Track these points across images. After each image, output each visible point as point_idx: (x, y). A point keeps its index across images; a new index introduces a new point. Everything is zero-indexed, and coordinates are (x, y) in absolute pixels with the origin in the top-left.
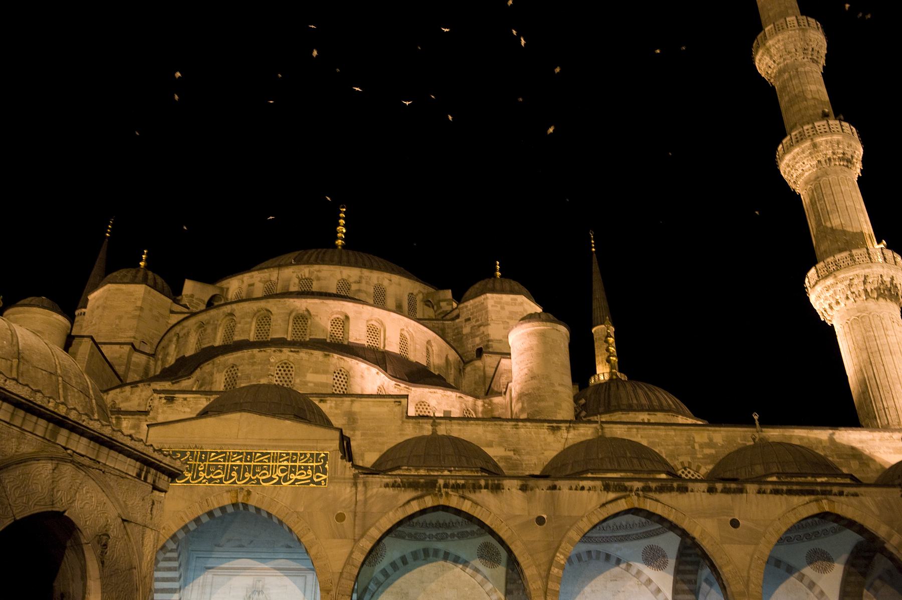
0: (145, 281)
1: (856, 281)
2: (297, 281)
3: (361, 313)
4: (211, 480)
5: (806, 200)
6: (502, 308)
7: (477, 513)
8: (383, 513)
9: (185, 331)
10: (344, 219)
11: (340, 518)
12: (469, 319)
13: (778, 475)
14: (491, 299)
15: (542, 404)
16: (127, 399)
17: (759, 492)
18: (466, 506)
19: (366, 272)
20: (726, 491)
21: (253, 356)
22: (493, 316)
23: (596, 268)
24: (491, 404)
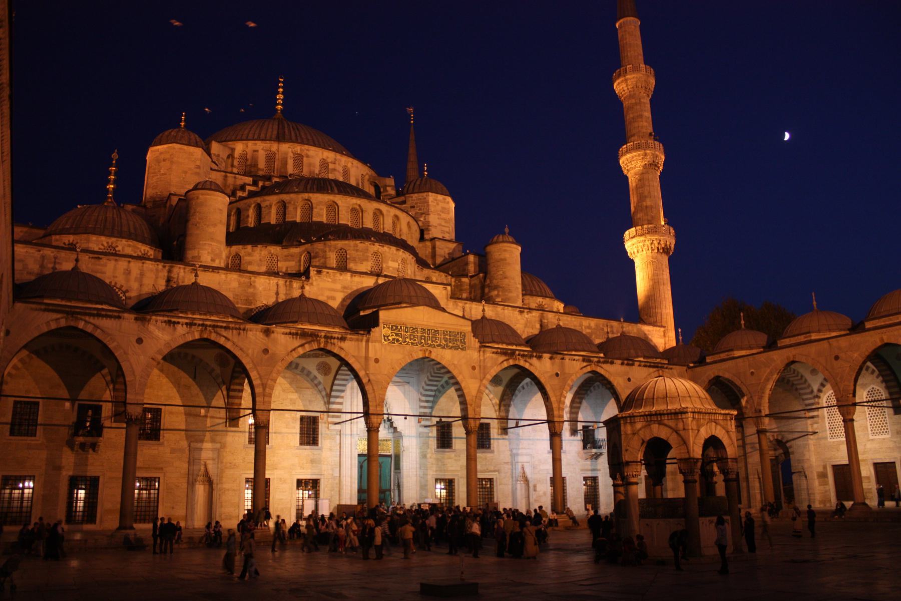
0: (196, 145)
1: (655, 242)
2: (291, 155)
3: (388, 211)
4: (412, 344)
5: (632, 182)
6: (438, 204)
7: (532, 369)
8: (492, 367)
9: (267, 203)
10: (282, 87)
11: (474, 368)
12: (413, 207)
13: (645, 357)
14: (432, 197)
15: (510, 295)
16: (249, 255)
17: (640, 366)
18: (527, 366)
19: (338, 156)
20: (628, 364)
21: (356, 246)
22: (432, 209)
23: (412, 137)
24: (460, 281)
